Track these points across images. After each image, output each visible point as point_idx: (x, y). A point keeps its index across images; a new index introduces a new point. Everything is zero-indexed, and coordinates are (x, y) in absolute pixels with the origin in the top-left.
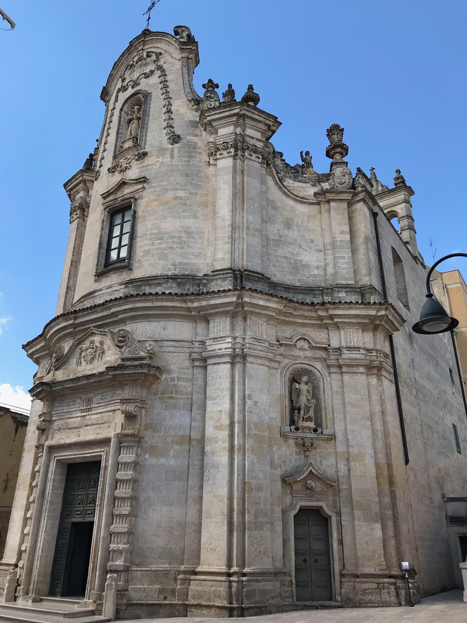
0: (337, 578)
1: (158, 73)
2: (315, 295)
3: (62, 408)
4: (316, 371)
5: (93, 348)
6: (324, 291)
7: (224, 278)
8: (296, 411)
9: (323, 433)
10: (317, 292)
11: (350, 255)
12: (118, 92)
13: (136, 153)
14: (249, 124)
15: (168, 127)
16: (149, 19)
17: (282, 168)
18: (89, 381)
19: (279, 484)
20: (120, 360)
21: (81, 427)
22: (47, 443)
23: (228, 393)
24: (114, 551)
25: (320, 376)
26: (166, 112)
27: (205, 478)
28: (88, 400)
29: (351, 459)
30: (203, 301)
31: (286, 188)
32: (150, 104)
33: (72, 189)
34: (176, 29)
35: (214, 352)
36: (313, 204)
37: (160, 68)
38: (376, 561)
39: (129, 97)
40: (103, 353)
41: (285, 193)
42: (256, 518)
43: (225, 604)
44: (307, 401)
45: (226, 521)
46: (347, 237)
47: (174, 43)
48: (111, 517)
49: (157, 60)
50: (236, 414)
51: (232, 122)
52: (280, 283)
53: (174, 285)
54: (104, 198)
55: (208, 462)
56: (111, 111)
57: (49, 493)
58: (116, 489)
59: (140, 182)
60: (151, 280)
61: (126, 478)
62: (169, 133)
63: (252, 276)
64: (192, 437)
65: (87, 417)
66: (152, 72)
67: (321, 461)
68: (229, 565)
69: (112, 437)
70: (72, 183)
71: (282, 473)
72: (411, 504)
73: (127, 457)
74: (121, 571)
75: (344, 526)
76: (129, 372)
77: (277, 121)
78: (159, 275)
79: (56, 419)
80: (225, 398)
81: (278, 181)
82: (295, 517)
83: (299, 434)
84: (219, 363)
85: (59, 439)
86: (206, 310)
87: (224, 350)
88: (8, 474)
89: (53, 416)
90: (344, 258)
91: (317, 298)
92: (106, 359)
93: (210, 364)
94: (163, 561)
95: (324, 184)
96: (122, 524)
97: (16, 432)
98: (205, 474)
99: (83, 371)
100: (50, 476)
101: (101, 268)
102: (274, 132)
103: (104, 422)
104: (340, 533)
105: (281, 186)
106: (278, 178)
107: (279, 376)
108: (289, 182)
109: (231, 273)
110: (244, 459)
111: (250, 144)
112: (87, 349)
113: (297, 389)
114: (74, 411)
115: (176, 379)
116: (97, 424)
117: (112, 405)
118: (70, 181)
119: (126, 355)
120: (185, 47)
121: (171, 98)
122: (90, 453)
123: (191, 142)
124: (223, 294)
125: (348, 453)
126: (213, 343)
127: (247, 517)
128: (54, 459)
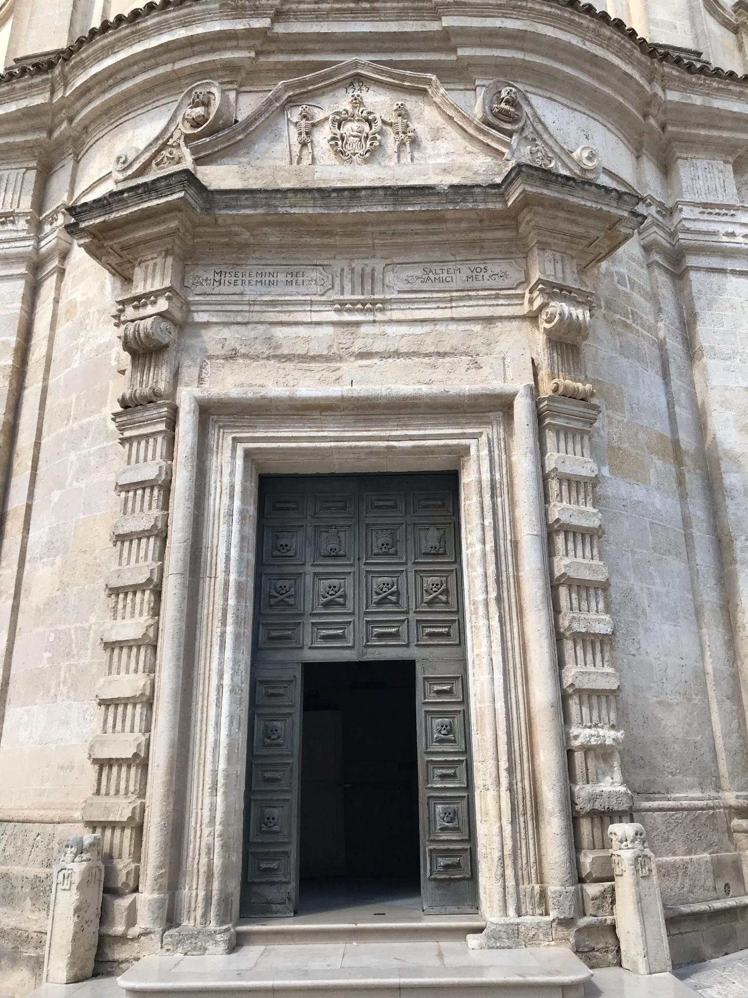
5: (370, 123)
18: (402, 208)
21: (341, 359)
24: (587, 749)
30: (695, 93)
35: (714, 238)
55: (740, 514)
65: (363, 329)
76: (582, 203)
79: (214, 320)
84: (722, 271)
86: (685, 124)
93: (698, 269)
103: (448, 350)
114: (304, 303)
117: (481, 302)
126: (701, 217)
128: (234, 449)
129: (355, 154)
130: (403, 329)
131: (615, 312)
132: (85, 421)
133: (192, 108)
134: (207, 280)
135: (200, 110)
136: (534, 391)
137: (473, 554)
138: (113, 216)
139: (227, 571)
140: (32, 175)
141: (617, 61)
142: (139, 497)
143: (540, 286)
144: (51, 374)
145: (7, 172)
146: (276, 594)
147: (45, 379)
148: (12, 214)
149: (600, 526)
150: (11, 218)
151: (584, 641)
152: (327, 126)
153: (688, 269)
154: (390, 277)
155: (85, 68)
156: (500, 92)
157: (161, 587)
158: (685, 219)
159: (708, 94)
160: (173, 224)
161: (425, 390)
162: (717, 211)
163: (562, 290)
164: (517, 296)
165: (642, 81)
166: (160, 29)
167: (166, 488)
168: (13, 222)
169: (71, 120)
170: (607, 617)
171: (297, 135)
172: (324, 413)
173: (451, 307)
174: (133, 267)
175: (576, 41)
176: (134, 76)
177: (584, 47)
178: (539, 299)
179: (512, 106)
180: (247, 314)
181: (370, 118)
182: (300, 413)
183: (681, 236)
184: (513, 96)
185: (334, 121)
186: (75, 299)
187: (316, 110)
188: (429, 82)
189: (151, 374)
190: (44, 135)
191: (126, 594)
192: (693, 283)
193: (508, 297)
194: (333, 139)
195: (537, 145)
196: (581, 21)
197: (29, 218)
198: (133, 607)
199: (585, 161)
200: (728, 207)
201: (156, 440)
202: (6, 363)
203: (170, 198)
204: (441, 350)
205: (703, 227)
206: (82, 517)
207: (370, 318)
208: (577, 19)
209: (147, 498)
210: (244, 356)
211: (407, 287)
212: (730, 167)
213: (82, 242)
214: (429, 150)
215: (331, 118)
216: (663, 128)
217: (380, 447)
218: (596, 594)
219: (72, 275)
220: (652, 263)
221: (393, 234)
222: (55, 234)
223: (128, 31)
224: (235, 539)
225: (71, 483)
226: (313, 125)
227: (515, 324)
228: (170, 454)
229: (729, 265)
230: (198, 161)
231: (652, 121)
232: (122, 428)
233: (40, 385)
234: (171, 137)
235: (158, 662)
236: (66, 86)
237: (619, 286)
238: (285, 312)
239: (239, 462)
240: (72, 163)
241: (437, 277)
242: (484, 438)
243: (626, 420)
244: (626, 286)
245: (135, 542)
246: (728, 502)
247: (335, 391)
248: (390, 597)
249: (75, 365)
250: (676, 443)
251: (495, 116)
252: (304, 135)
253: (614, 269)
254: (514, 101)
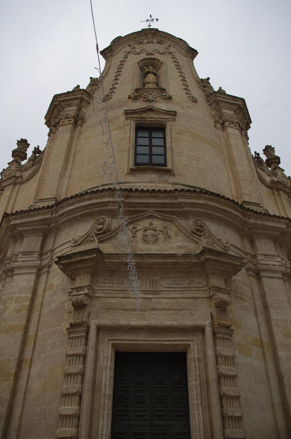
3: (111, 285)
5: (155, 231)
35: (269, 266)
51: (233, 108)
57: (105, 384)
59: (170, 115)
61: (230, 373)
65: (153, 300)
70: (60, 98)
76: (225, 261)
79: (103, 296)
80: (287, 310)
84: (273, 277)
87: (278, 267)
89: (96, 291)
93: (265, 277)
101: (131, 165)
116: (170, 309)
117: (193, 292)
122: (170, 341)
124: (276, 219)
126: (264, 259)
128: (108, 343)
129: (150, 241)
130: (166, 301)
132: (55, 328)
133: (98, 225)
134: (100, 282)
135: (101, 226)
136: (212, 324)
137: (192, 385)
138: (72, 260)
140: (41, 238)
141: (233, 211)
142: (75, 360)
143: (212, 288)
144: (42, 309)
145: (32, 237)
146: (120, 398)
147: (40, 311)
148: (33, 252)
149: (236, 375)
150: (33, 253)
151: (232, 419)
152: (141, 231)
153: (261, 277)
154: (162, 282)
155: (63, 208)
156: (197, 223)
157: (82, 394)
158: (259, 259)
159: (263, 220)
160: (92, 264)
161: (175, 323)
162: (269, 257)
163: (219, 289)
164: (205, 290)
165: (242, 217)
166: (89, 199)
167: (85, 357)
168: (33, 254)
169: (56, 223)
170: (240, 410)
171: (131, 234)
172: (140, 331)
173: (183, 294)
174: (76, 276)
175: (220, 206)
176: (79, 212)
177: (223, 208)
178: (212, 292)
179: (201, 227)
180: (114, 294)
181: (155, 229)
182: (131, 330)
183: (258, 265)
184: (201, 224)
185: (144, 230)
186: (53, 283)
187: (138, 226)
188: (174, 218)
189: (81, 315)
190: (47, 226)
191: (69, 396)
192: (263, 282)
193: (202, 290)
194: (143, 236)
195: (209, 239)
196: (221, 200)
197: (39, 253)
198: (71, 402)
199: (225, 244)
200: (273, 256)
201: (81, 339)
202: (27, 304)
203: (91, 256)
204: (180, 309)
205: (266, 262)
206: (52, 364)
208: (220, 200)
209: (77, 360)
210: (112, 309)
211: (168, 286)
212: (272, 242)
213: (60, 267)
214: (174, 240)
215: (143, 229)
216: (250, 229)
217: (159, 344)
218: (236, 400)
219: (52, 274)
220: (249, 275)
221: (163, 268)
222: (48, 260)
223: (79, 199)
224: (108, 377)
225: (49, 351)
226: (137, 231)
227: (204, 299)
228: (86, 344)
229: (275, 275)
230: (99, 242)
231: (246, 228)
232: (69, 333)
233: (39, 313)
234: (91, 233)
235: (80, 423)
236: (56, 213)
237: (238, 284)
238: (126, 294)
239: (110, 348)
240: (54, 235)
241: (178, 283)
242: (195, 341)
243: (243, 333)
244: (241, 284)
245: (73, 377)
246: (281, 362)
247: (143, 323)
248: (162, 401)
249: (52, 307)
250: (261, 340)
251: (196, 230)
252: (134, 234)
253: (236, 278)
254: (201, 225)
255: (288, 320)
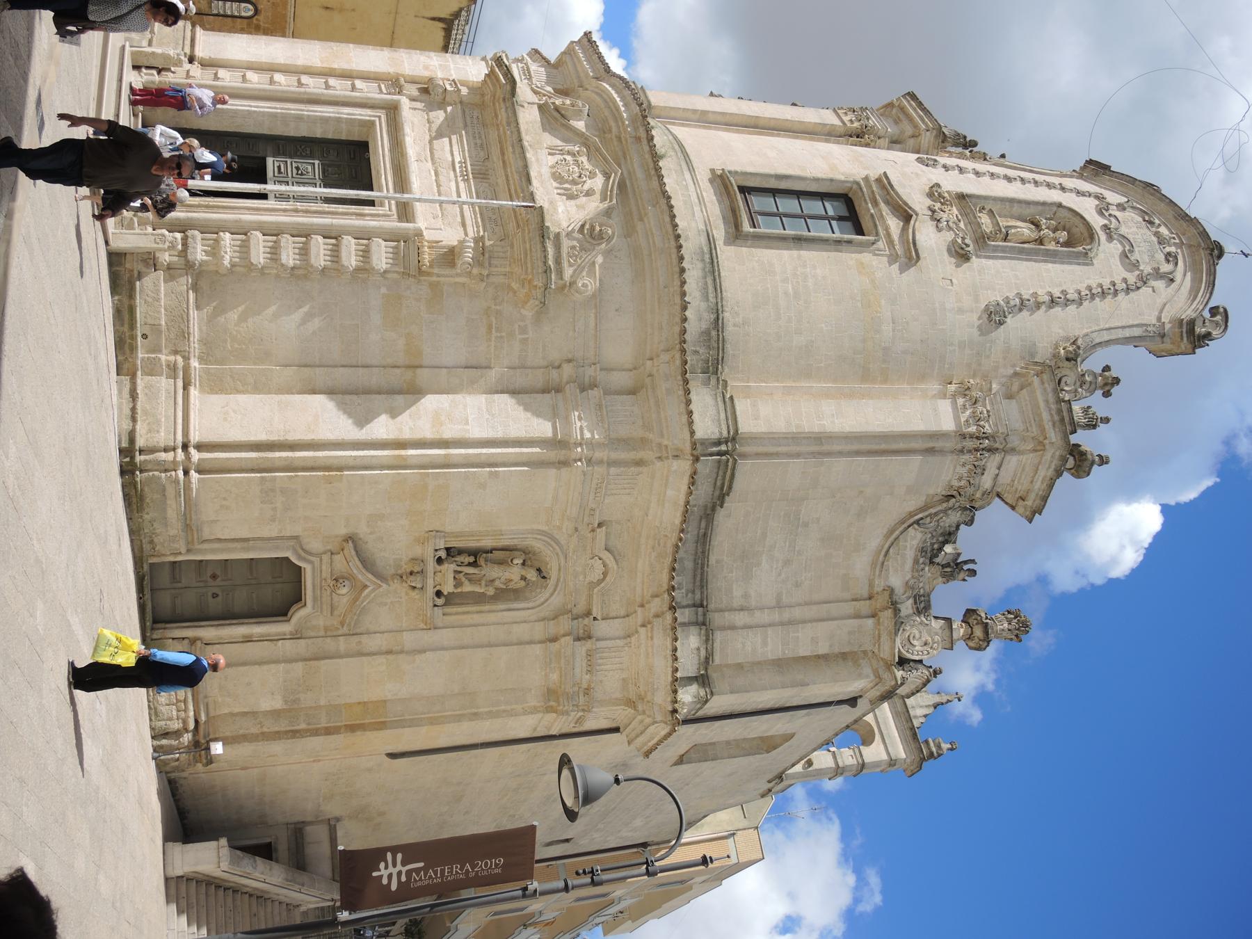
0: (189, 633)
1: (1132, 278)
2: (693, 592)
4: (548, 595)
6: (700, 610)
7: (719, 420)
8: (472, 559)
9: (436, 608)
10: (698, 596)
11: (770, 657)
12: (1099, 197)
13: (967, 241)
14: (1027, 459)
15: (1022, 301)
16: (1244, 254)
17: (942, 524)
19: (343, 531)
20: (557, 231)
22: (405, 103)
23: (499, 434)
24: (217, 241)
25: (538, 602)
26: (1051, 296)
27: (348, 397)
28: (484, 174)
29: (390, 657)
31: (902, 533)
32: (1071, 263)
33: (902, 109)
34: (1222, 310)
36: (871, 585)
37: (1144, 280)
38: (220, 699)
39: (1085, 219)
40: (571, 197)
41: (891, 532)
42: (281, 492)
43: (140, 442)
44: (491, 579)
45: (274, 438)
46: (804, 651)
47: (1193, 307)
48: (275, 232)
49: (1157, 274)
50: (463, 451)
51: (1031, 426)
52: (714, 527)
53: (704, 326)
54: (878, 180)
56: (1060, 184)
58: (324, 238)
60: (715, 280)
62: (1008, 303)
63: (725, 473)
64: (419, 371)
65: (452, 173)
66: (1135, 265)
67: (386, 604)
68: (200, 447)
69: (416, 225)
71: (362, 536)
72: (319, 761)
73: (381, 256)
74: (186, 256)
75: (276, 645)
77: (1034, 513)
78: (724, 294)
81: (917, 517)
82: (287, 559)
83: (432, 564)
85: (413, 123)
88: (353, 10)
90: (765, 644)
91: (687, 595)
92: (560, 203)
94: (204, 328)
95: (910, 607)
96: (264, 253)
97: (434, 19)
98: (354, 397)
99: (537, 160)
100: (346, 112)
102: (1013, 508)
104: (262, 639)
105: (906, 525)
106: (922, 519)
107: (535, 527)
108: (915, 538)
109: (729, 432)
110: (382, 467)
111: (986, 462)
112: (579, 166)
113: (512, 561)
115: (523, 336)
118: (920, 104)
119: (566, 244)
120: (1184, 330)
121: (1081, 304)
123: (991, 346)
125: (402, 652)
127: (282, 474)
130: (454, 189)
131: (496, 318)
139: (308, 111)
188: (611, 201)
207: (458, 174)
255: (468, 427)
